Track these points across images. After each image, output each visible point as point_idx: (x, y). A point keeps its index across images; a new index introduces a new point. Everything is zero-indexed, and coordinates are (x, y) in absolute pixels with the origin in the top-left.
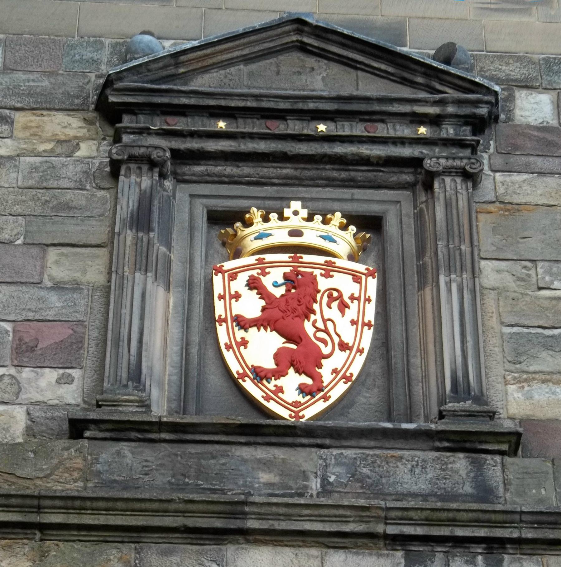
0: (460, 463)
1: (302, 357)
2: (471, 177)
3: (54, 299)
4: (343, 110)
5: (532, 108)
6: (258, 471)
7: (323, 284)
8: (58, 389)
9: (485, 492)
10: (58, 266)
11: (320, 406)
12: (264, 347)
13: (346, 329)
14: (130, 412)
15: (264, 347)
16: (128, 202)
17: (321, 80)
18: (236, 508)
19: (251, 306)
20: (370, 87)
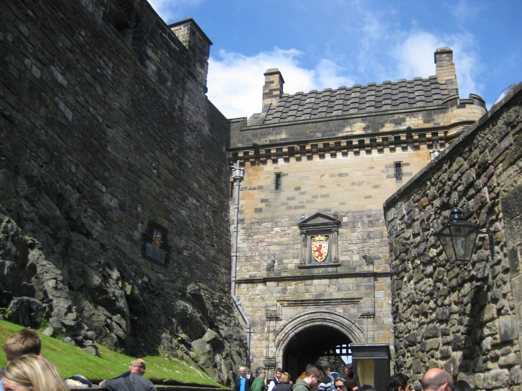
0: (335, 268)
1: (321, 255)
2: (338, 232)
3: (296, 251)
4: (323, 224)
5: (345, 219)
6: (316, 271)
7: (323, 245)
8: (297, 261)
9: (337, 271)
10: (296, 246)
11: (322, 260)
12: (317, 253)
13: (325, 250)
14: (303, 265)
15: (317, 253)
16: (302, 239)
17: (321, 220)
18: (313, 276)
19: (315, 249)
20: (326, 221)
